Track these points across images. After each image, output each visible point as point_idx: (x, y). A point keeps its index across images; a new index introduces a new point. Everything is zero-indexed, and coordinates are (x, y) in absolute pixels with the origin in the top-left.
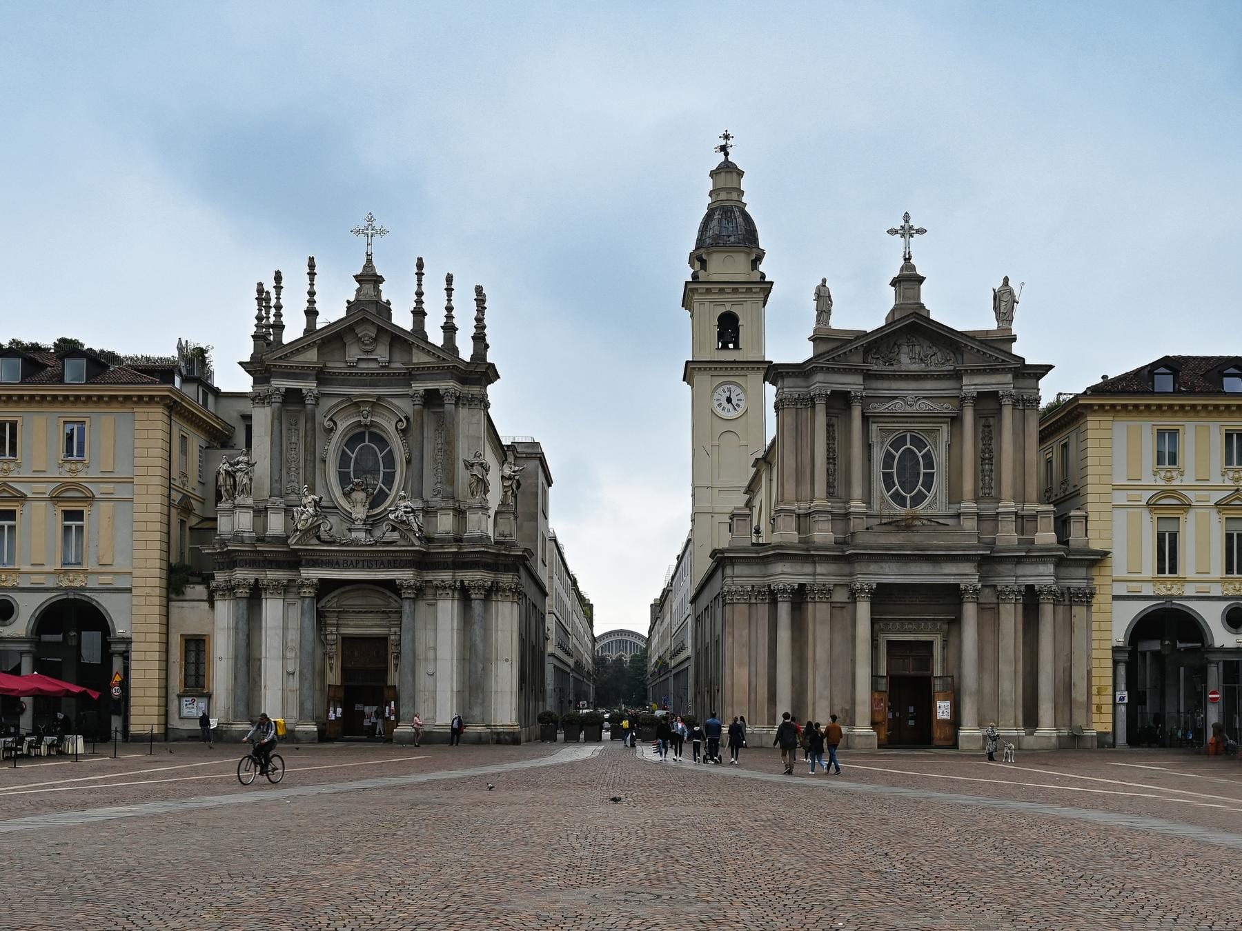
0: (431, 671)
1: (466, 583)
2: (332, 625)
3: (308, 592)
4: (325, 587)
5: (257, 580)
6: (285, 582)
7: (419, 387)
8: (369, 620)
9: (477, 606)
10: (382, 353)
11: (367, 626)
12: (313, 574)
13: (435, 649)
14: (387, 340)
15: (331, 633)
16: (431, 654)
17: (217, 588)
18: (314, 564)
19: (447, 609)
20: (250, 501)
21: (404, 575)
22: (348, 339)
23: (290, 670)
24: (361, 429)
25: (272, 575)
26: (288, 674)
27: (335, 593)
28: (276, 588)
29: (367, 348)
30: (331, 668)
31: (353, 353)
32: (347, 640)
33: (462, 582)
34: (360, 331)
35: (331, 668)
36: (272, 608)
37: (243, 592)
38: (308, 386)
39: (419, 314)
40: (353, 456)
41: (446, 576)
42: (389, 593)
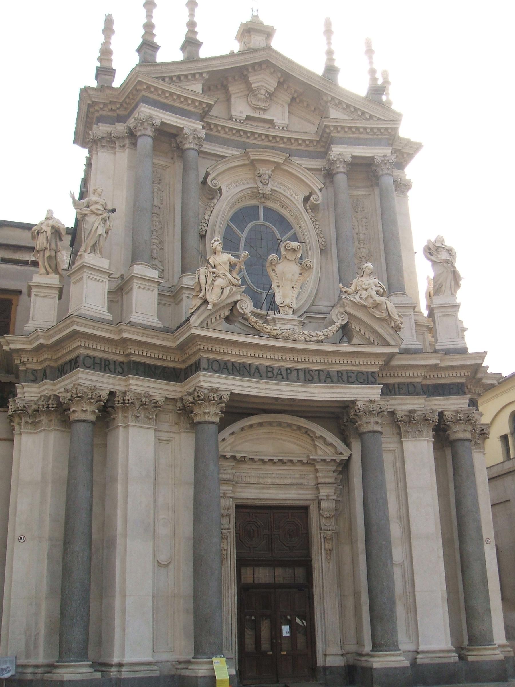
1: (448, 414)
3: (212, 414)
4: (238, 410)
5: (112, 394)
6: (160, 399)
8: (294, 474)
10: (278, 114)
11: (280, 486)
14: (285, 98)
17: (22, 412)
20: (104, 264)
21: (365, 394)
23: (163, 558)
25: (138, 385)
26: (159, 564)
29: (261, 104)
32: (249, 514)
33: (441, 414)
34: (257, 80)
36: (137, 445)
37: (85, 412)
38: (191, 126)
40: (244, 236)
41: (417, 403)
42: (319, 430)
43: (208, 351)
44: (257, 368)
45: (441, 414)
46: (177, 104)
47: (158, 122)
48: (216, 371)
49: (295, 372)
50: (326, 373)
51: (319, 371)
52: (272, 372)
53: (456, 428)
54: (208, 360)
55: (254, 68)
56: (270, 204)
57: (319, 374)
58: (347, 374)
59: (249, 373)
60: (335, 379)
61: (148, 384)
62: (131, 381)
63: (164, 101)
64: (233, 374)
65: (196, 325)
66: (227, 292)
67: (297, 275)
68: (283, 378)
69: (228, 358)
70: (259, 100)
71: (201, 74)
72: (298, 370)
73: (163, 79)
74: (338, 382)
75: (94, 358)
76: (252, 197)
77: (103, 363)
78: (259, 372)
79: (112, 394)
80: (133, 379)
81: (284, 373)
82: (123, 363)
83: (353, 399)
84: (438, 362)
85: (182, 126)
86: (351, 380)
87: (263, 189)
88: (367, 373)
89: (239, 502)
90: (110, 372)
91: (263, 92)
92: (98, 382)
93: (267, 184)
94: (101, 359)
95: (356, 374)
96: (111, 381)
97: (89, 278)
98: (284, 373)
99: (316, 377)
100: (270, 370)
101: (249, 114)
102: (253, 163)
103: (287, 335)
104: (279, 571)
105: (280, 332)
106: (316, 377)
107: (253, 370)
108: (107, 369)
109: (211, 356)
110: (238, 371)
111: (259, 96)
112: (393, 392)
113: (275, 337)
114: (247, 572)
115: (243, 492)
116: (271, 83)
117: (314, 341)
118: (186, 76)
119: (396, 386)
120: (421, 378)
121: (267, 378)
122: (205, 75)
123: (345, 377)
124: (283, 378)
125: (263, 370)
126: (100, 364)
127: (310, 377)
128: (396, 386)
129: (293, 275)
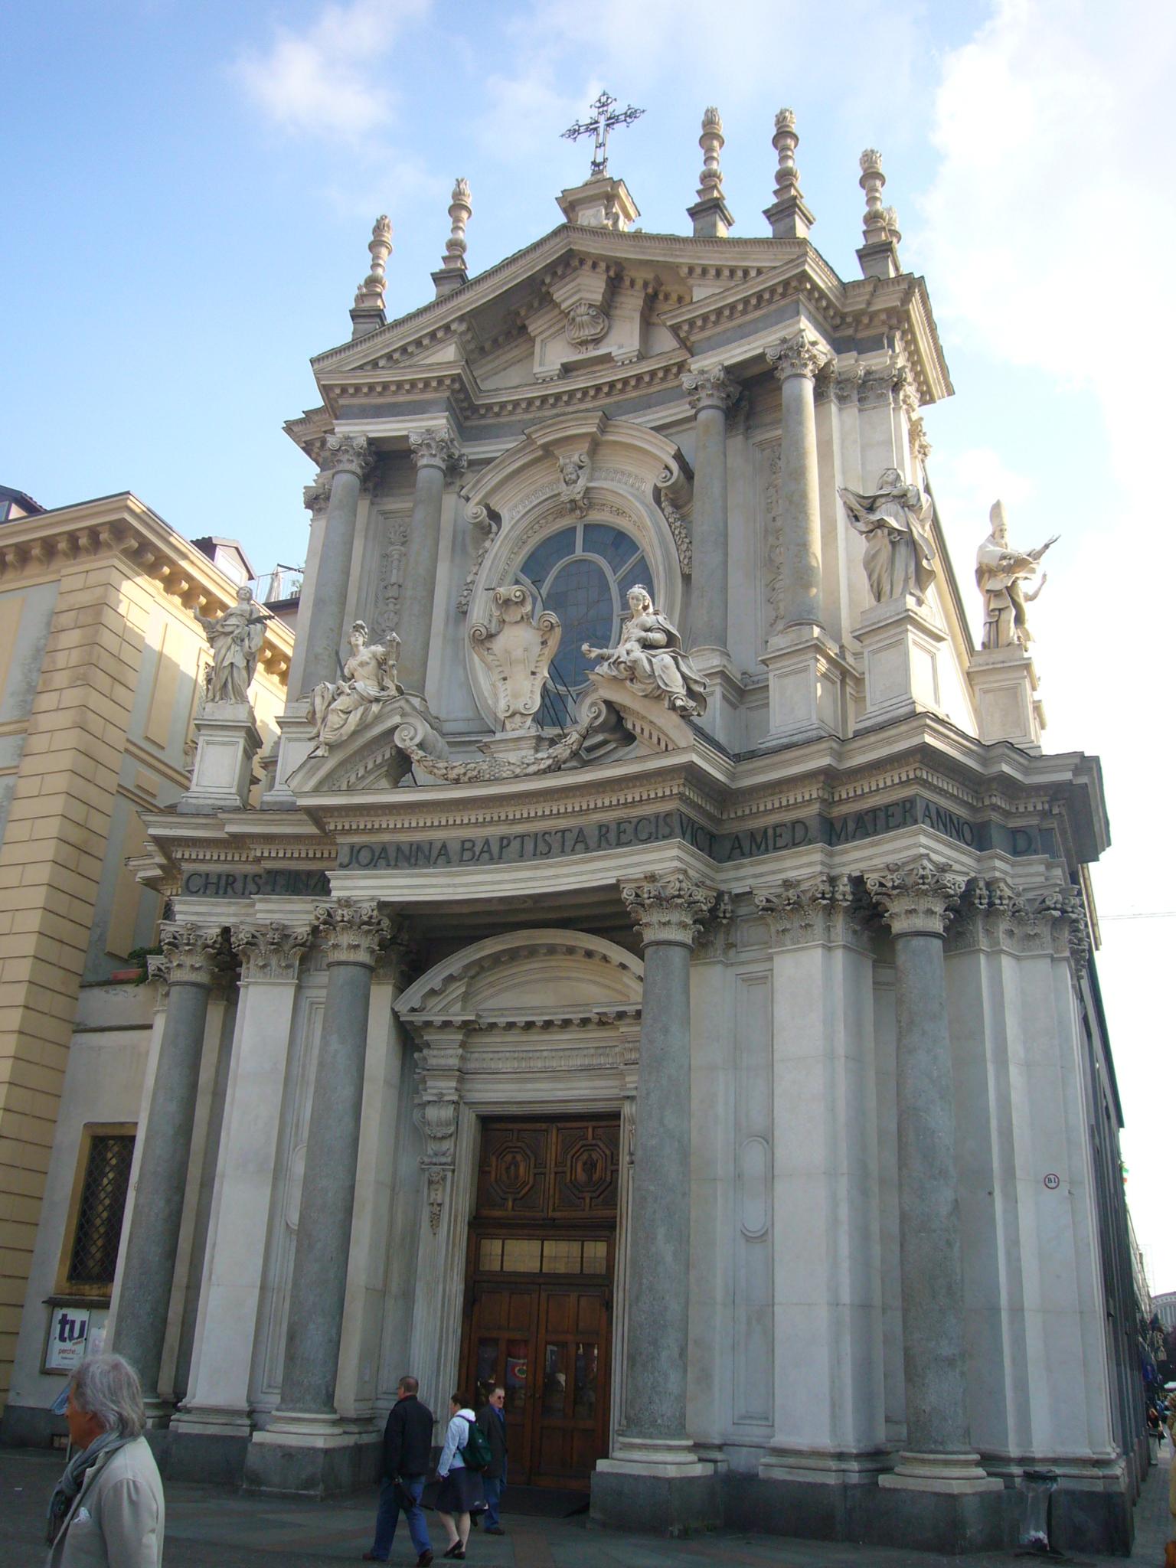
0: (755, 1225)
1: (872, 881)
2: (444, 1072)
3: (351, 947)
5: (226, 931)
7: (712, 362)
9: (923, 963)
11: (554, 1075)
12: (363, 888)
13: (767, 1138)
15: (439, 1101)
16: (754, 1160)
18: (381, 858)
19: (809, 982)
22: (536, 326)
24: (565, 522)
27: (454, 964)
28: (277, 946)
29: (587, 333)
30: (435, 1220)
31: (553, 354)
32: (499, 1130)
33: (858, 882)
35: (435, 1220)
37: (189, 969)
39: (708, 208)
41: (804, 865)
43: (349, 832)
44: (444, 846)
45: (858, 882)
46: (401, 398)
47: (362, 441)
48: (366, 866)
49: (516, 845)
50: (575, 832)
51: (563, 832)
52: (471, 849)
53: (896, 907)
54: (352, 847)
55: (594, 266)
56: (596, 516)
57: (563, 837)
58: (619, 828)
59: (428, 858)
60: (593, 842)
61: (289, 907)
62: (259, 906)
63: (380, 400)
64: (396, 867)
65: (308, 787)
66: (354, 719)
67: (536, 649)
68: (492, 859)
69: (386, 838)
70: (581, 326)
71: (447, 327)
72: (522, 837)
73: (374, 364)
74: (599, 848)
75: (207, 875)
76: (560, 513)
77: (223, 882)
78: (446, 854)
79: (226, 931)
80: (260, 900)
81: (495, 849)
82: (260, 876)
83: (613, 881)
84: (826, 761)
85: (405, 433)
86: (624, 838)
87: (568, 493)
88: (657, 816)
89: (486, 1110)
90: (235, 895)
91: (583, 310)
92: (210, 914)
93: (575, 482)
94: (219, 876)
95: (633, 825)
96: (232, 909)
97: (208, 743)
98: (495, 849)
99: (556, 847)
100: (467, 846)
101: (565, 360)
102: (548, 451)
103: (475, 773)
104: (550, 1248)
105: (463, 771)
106: (556, 847)
107: (435, 853)
108: (229, 890)
109: (356, 839)
110: (408, 859)
111: (578, 319)
112: (763, 846)
113: (457, 781)
114: (493, 1247)
115: (487, 1091)
116: (592, 287)
117: (535, 774)
118: (418, 343)
119: (770, 832)
120: (817, 806)
121: (462, 862)
122: (454, 327)
123: (612, 836)
124: (492, 859)
125: (454, 848)
126: (218, 884)
127: (543, 847)
128: (770, 832)
129: (526, 650)
